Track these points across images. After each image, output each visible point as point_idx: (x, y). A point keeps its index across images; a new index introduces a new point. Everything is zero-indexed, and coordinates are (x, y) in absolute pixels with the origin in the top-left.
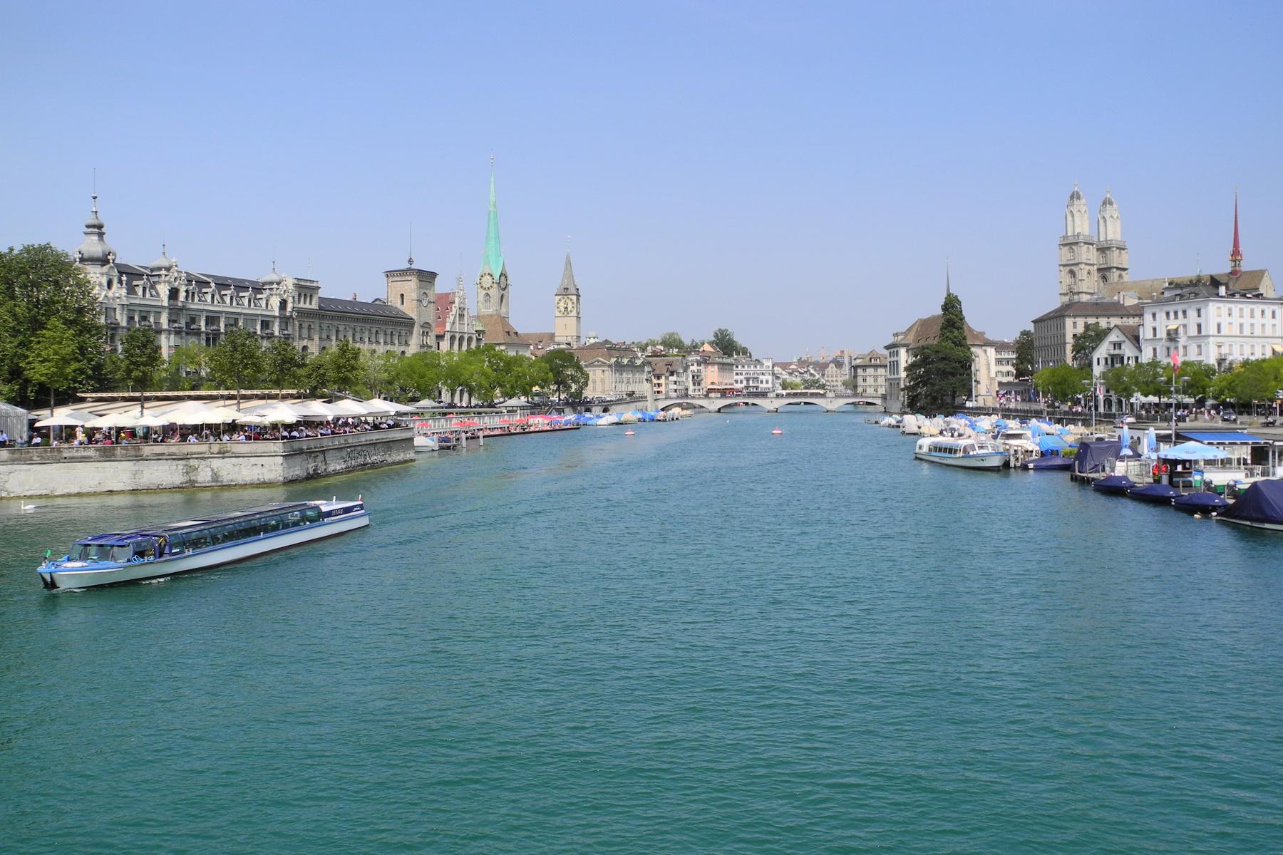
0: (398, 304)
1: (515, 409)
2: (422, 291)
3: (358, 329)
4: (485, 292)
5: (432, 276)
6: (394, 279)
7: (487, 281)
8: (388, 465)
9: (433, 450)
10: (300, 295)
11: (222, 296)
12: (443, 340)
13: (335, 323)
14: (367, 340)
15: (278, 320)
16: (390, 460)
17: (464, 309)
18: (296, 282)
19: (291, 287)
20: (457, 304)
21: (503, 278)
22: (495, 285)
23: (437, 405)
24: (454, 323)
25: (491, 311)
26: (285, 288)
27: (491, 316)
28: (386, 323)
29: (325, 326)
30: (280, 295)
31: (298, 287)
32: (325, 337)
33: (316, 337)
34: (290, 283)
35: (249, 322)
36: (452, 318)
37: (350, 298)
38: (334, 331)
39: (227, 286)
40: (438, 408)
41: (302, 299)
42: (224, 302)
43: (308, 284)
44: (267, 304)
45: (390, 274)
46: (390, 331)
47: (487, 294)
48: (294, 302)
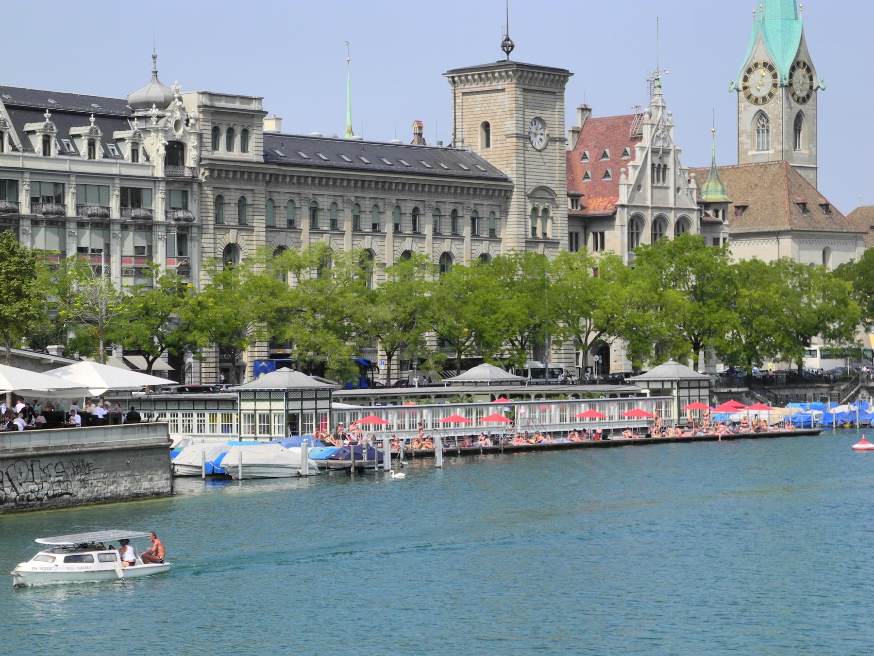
0: (475, 144)
1: (667, 386)
2: (531, 114)
3: (367, 205)
4: (756, 108)
5: (559, 77)
6: (469, 88)
7: (760, 82)
8: (77, 503)
9: (299, 476)
10: (216, 131)
11: (25, 137)
12: (612, 227)
13: (309, 192)
14: (388, 228)
15: (162, 186)
16: (81, 493)
17: (666, 152)
18: (205, 100)
19: (193, 112)
20: (646, 142)
21: (800, 72)
22: (780, 92)
23: (509, 376)
24: (638, 187)
25: (771, 154)
26: (178, 115)
27: (765, 166)
28: (438, 190)
29: (282, 199)
30: (165, 131)
31: (210, 111)
32: (281, 222)
33: (259, 223)
34: (192, 104)
35: (92, 193)
36: (633, 175)
37: (407, 138)
38: (306, 210)
39: (36, 113)
40: (511, 382)
41: (223, 140)
42: (28, 147)
43: (237, 105)
44: (135, 153)
45: (457, 76)
46: (412, 205)
47: (762, 115)
48: (201, 145)
